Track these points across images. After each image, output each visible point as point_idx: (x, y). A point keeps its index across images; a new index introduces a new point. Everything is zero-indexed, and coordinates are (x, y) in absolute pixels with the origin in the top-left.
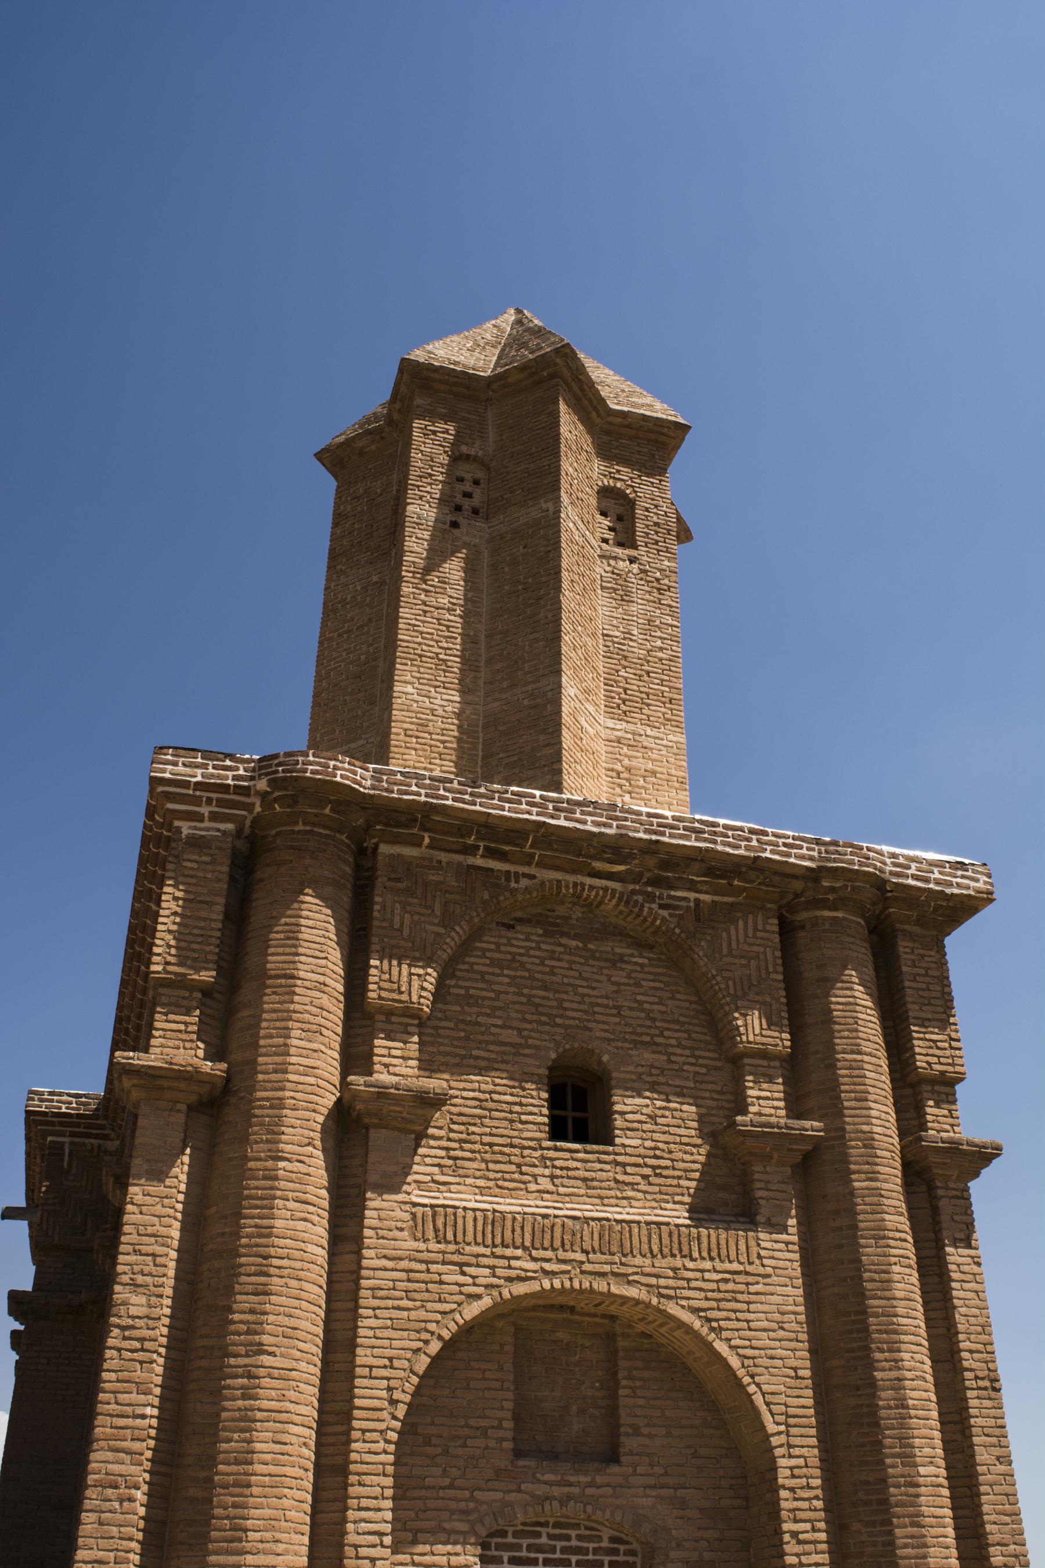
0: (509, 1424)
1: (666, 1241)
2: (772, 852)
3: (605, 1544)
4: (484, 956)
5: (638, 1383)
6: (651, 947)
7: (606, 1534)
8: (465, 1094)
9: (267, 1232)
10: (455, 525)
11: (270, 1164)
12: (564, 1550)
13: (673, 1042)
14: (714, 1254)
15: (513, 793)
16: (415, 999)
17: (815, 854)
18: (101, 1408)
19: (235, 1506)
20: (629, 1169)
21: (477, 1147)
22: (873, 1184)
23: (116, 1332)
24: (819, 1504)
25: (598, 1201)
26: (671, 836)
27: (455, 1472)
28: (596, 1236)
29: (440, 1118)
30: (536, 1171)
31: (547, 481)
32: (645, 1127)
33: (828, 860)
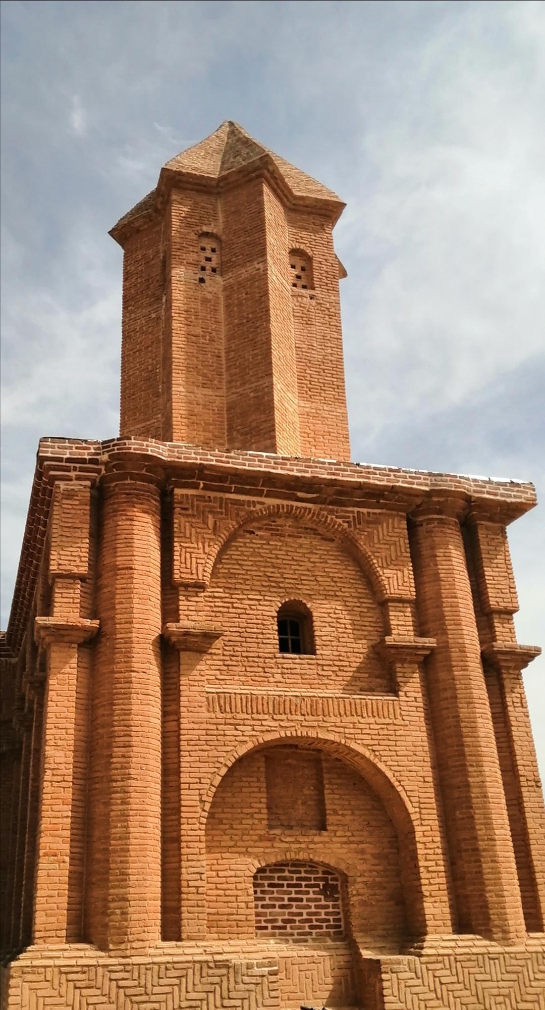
0: (265, 811)
1: (348, 707)
2: (403, 482)
3: (320, 875)
4: (237, 550)
5: (335, 787)
6: (332, 540)
7: (320, 869)
8: (231, 629)
9: (128, 713)
10: (202, 280)
11: (127, 675)
12: (298, 879)
13: (347, 594)
14: (375, 714)
15: (250, 455)
16: (200, 577)
17: (429, 482)
18: (43, 814)
19: (121, 862)
20: (325, 668)
21: (239, 658)
22: (465, 673)
23: (49, 772)
24: (439, 851)
25: (308, 686)
26: (343, 476)
27: (236, 838)
28: (309, 706)
29: (219, 643)
30: (273, 671)
31: (258, 250)
32: (333, 644)
33: (437, 485)
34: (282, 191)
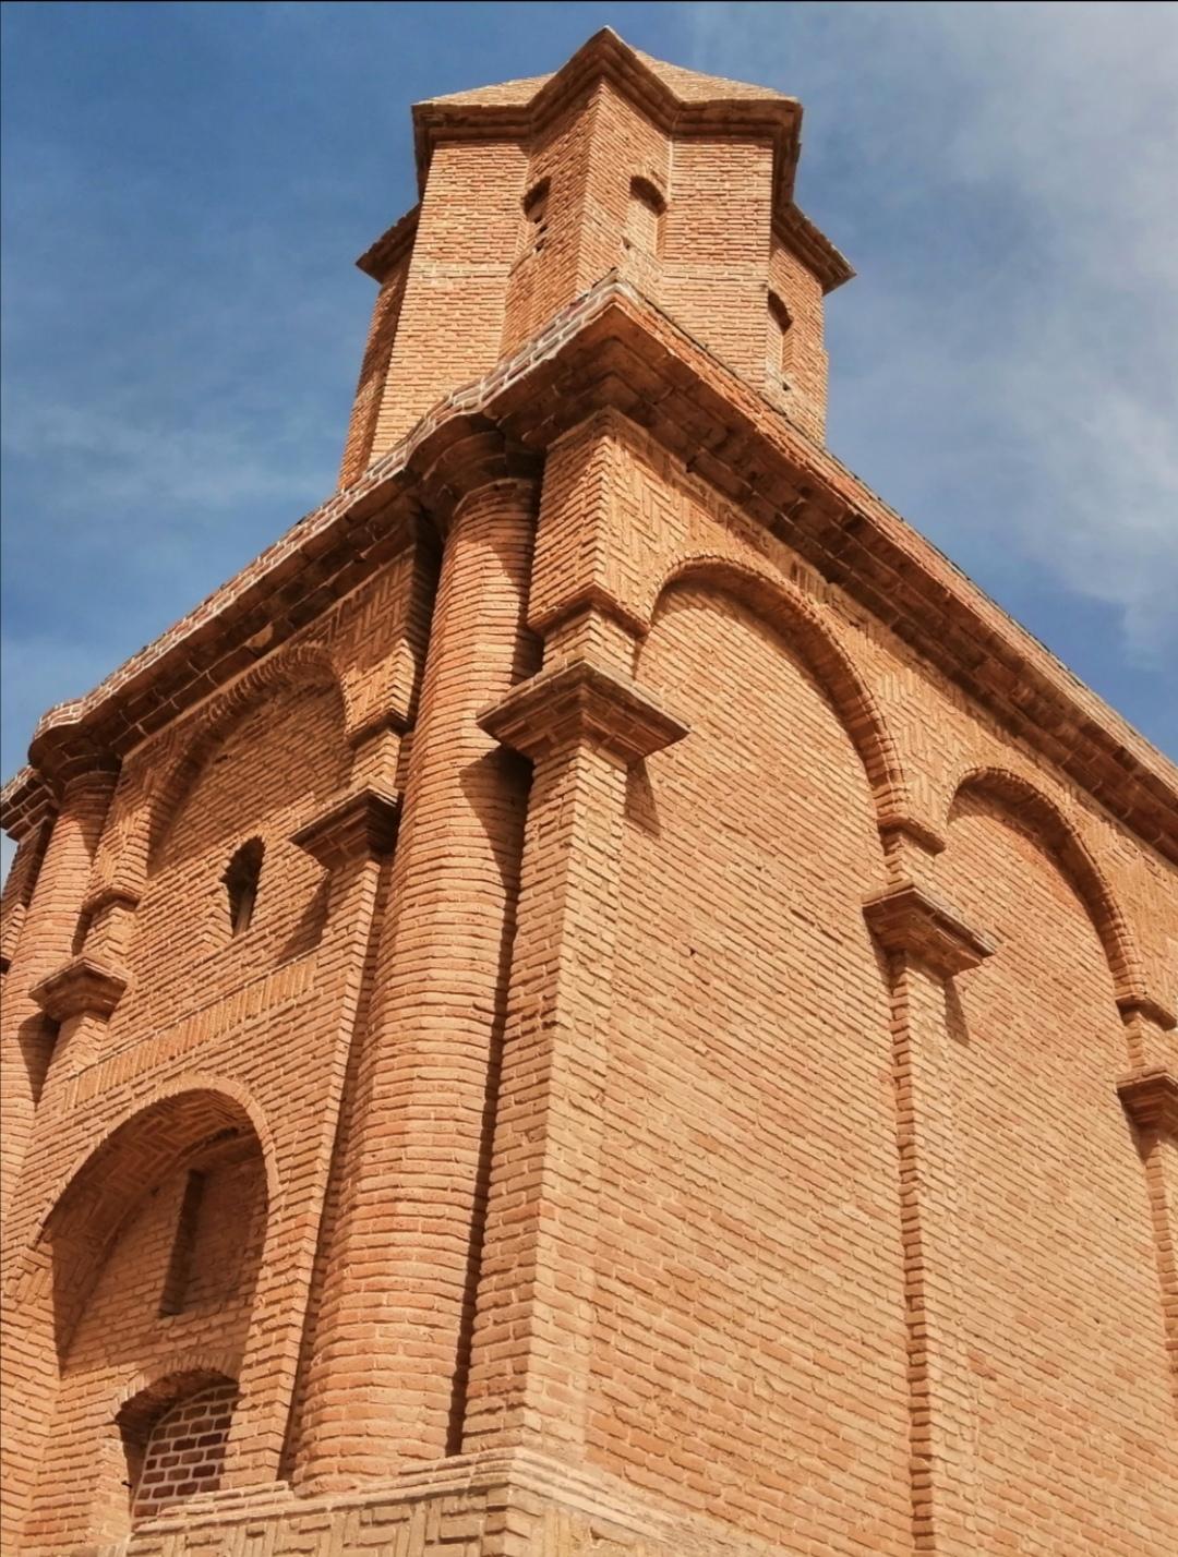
34: (495, 124)
